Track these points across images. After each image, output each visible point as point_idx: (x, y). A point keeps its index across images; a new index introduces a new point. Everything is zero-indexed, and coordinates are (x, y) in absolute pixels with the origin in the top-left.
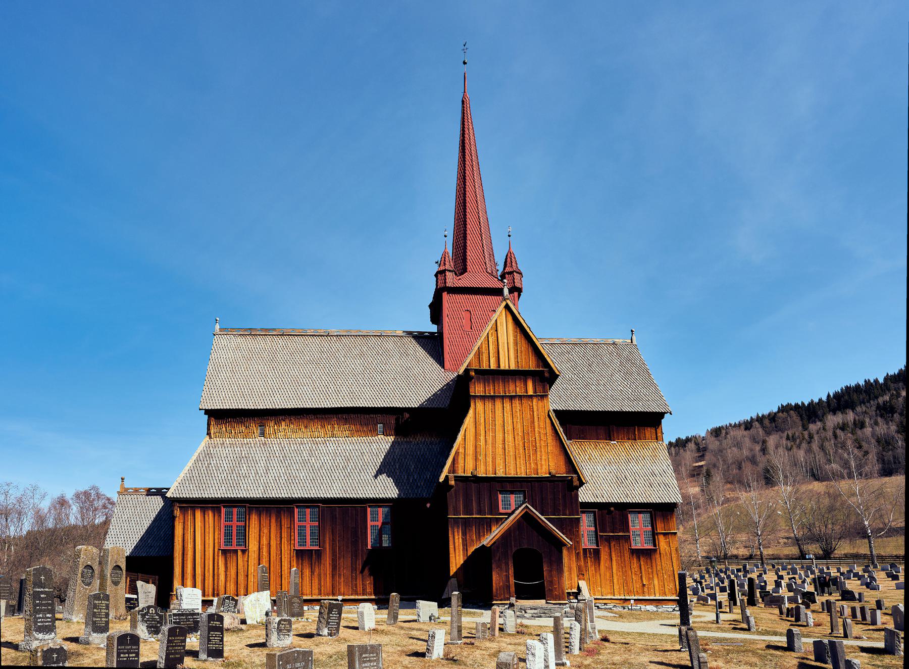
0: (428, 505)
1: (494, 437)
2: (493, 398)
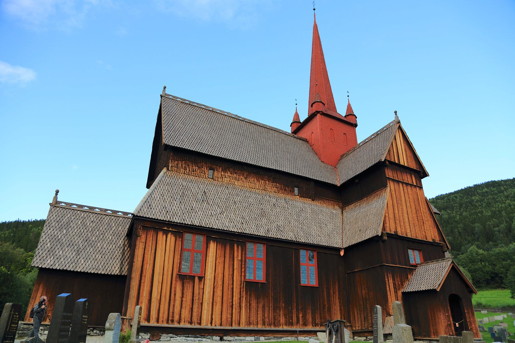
1: (402, 209)
2: (398, 182)
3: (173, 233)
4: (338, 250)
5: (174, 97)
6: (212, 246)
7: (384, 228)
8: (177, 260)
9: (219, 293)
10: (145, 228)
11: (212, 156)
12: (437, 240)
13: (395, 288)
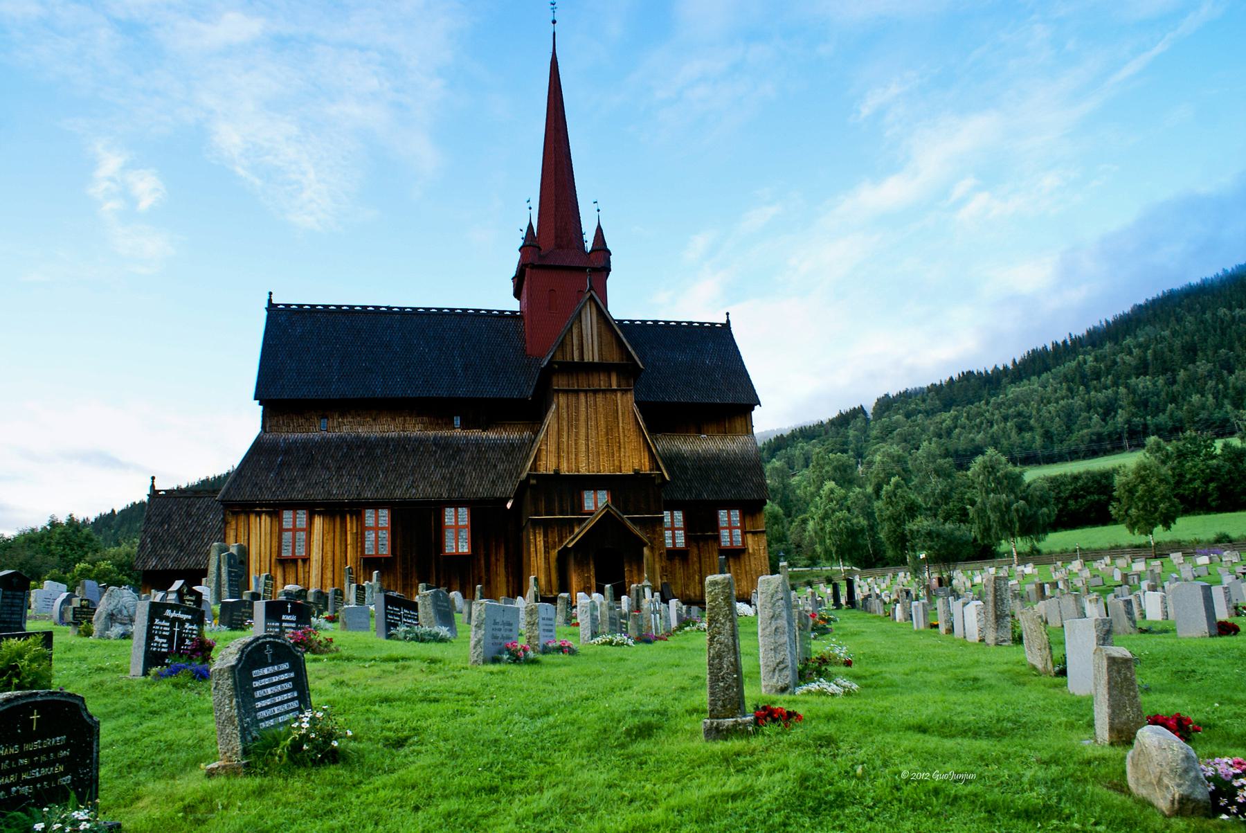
0: (509, 505)
3: (267, 513)
6: (318, 521)
8: (275, 544)
9: (329, 574)
10: (236, 514)
12: (646, 468)
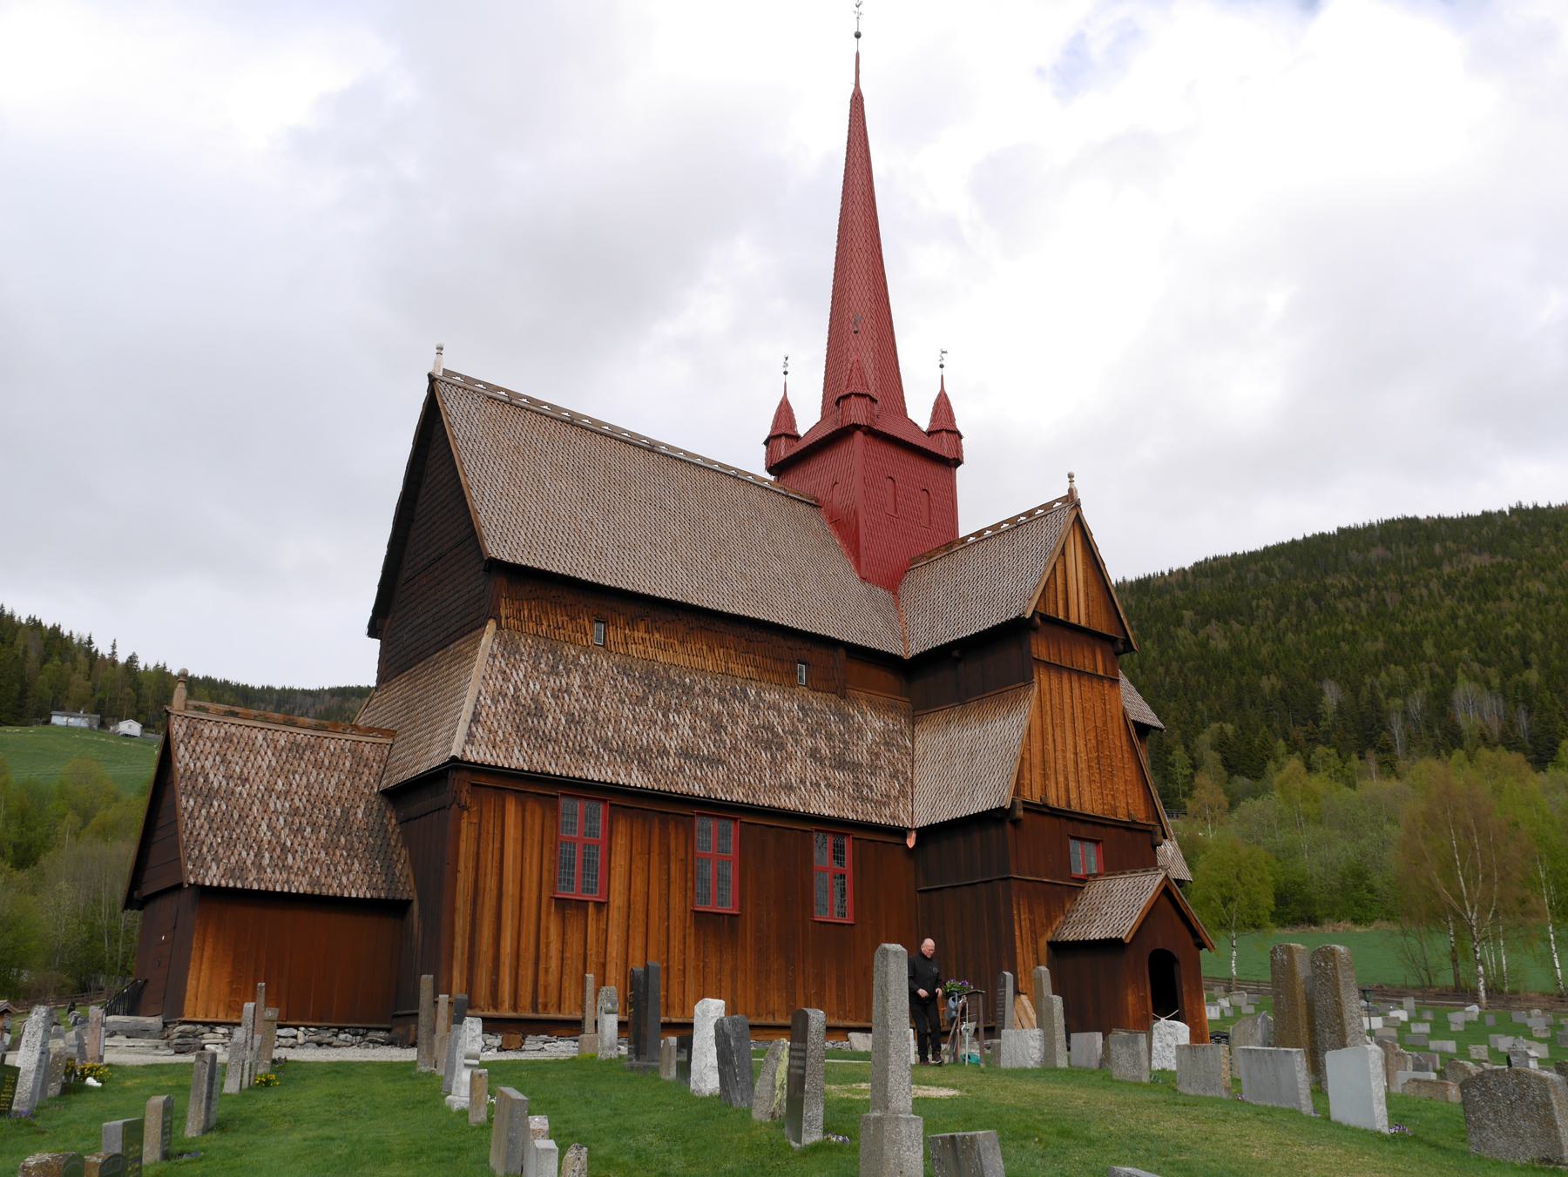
2: (1059, 668)
4: (902, 832)
5: (466, 379)
7: (1017, 791)
11: (603, 586)
12: (1141, 815)
13: (1033, 932)
